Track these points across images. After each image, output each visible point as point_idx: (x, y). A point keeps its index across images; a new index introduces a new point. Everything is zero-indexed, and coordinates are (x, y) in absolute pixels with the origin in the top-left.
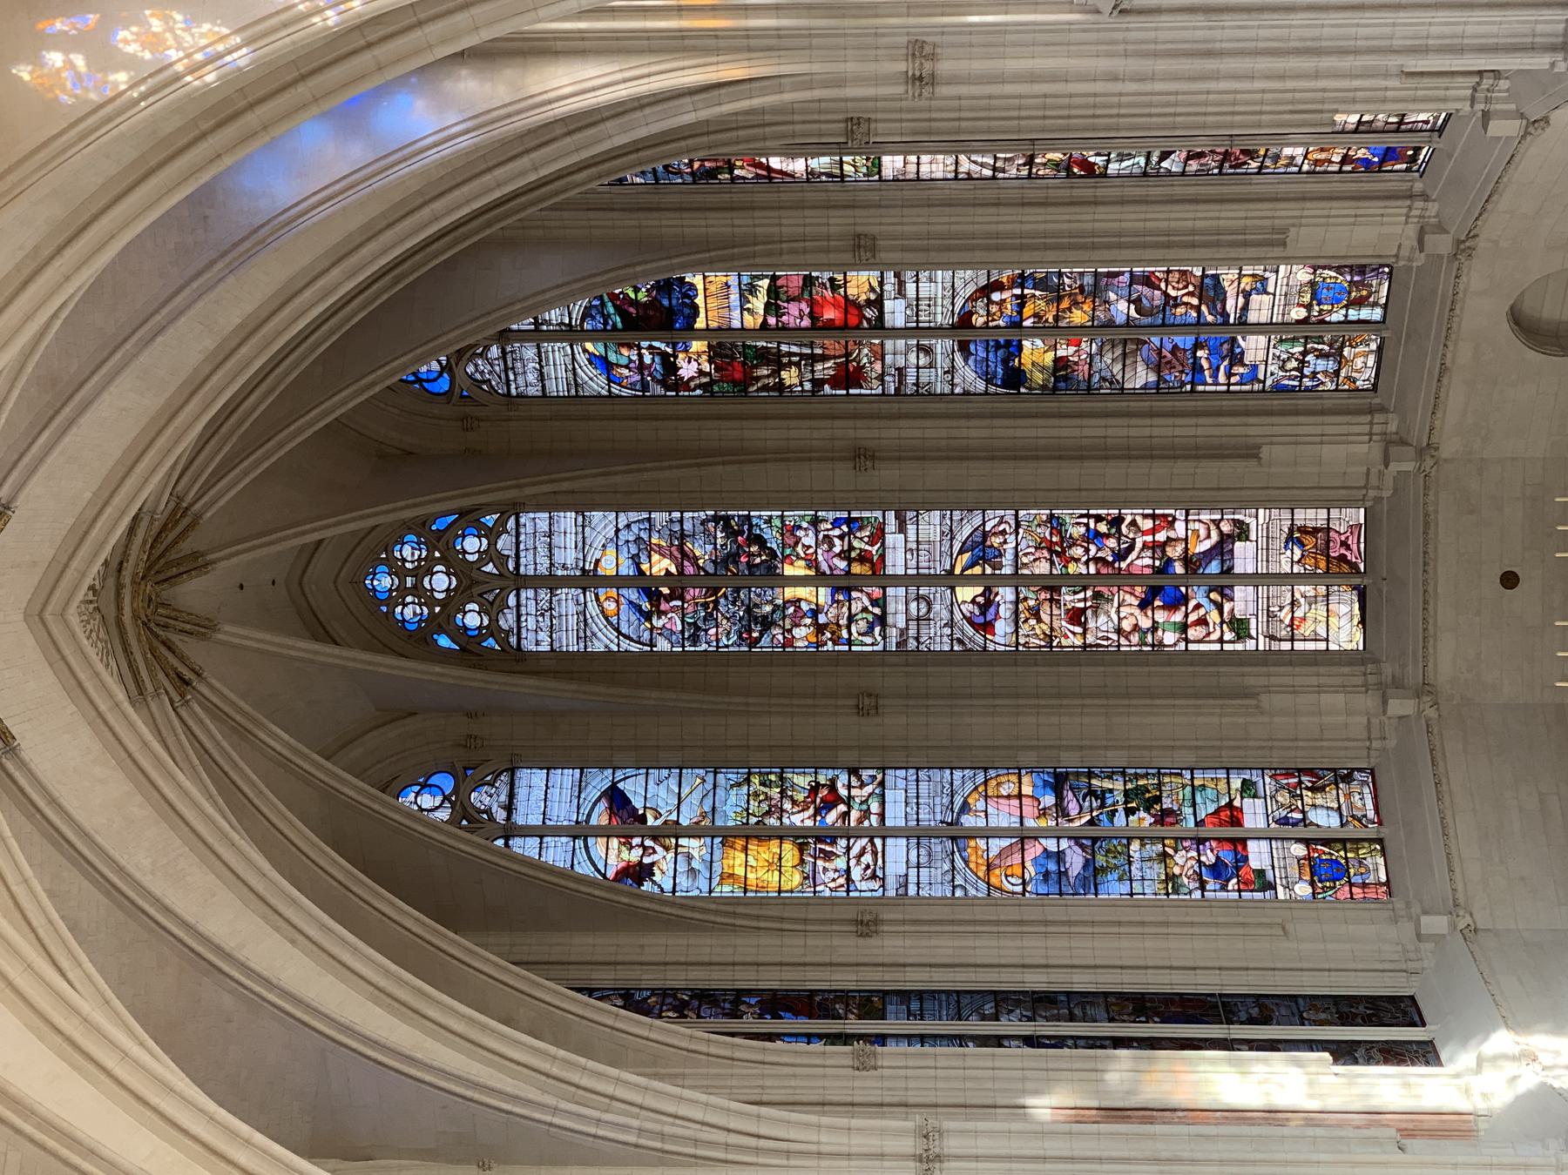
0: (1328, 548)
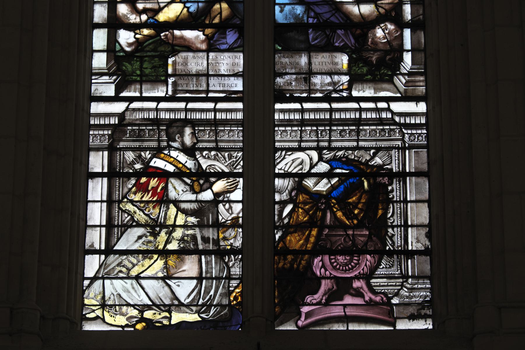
0: (333, 252)
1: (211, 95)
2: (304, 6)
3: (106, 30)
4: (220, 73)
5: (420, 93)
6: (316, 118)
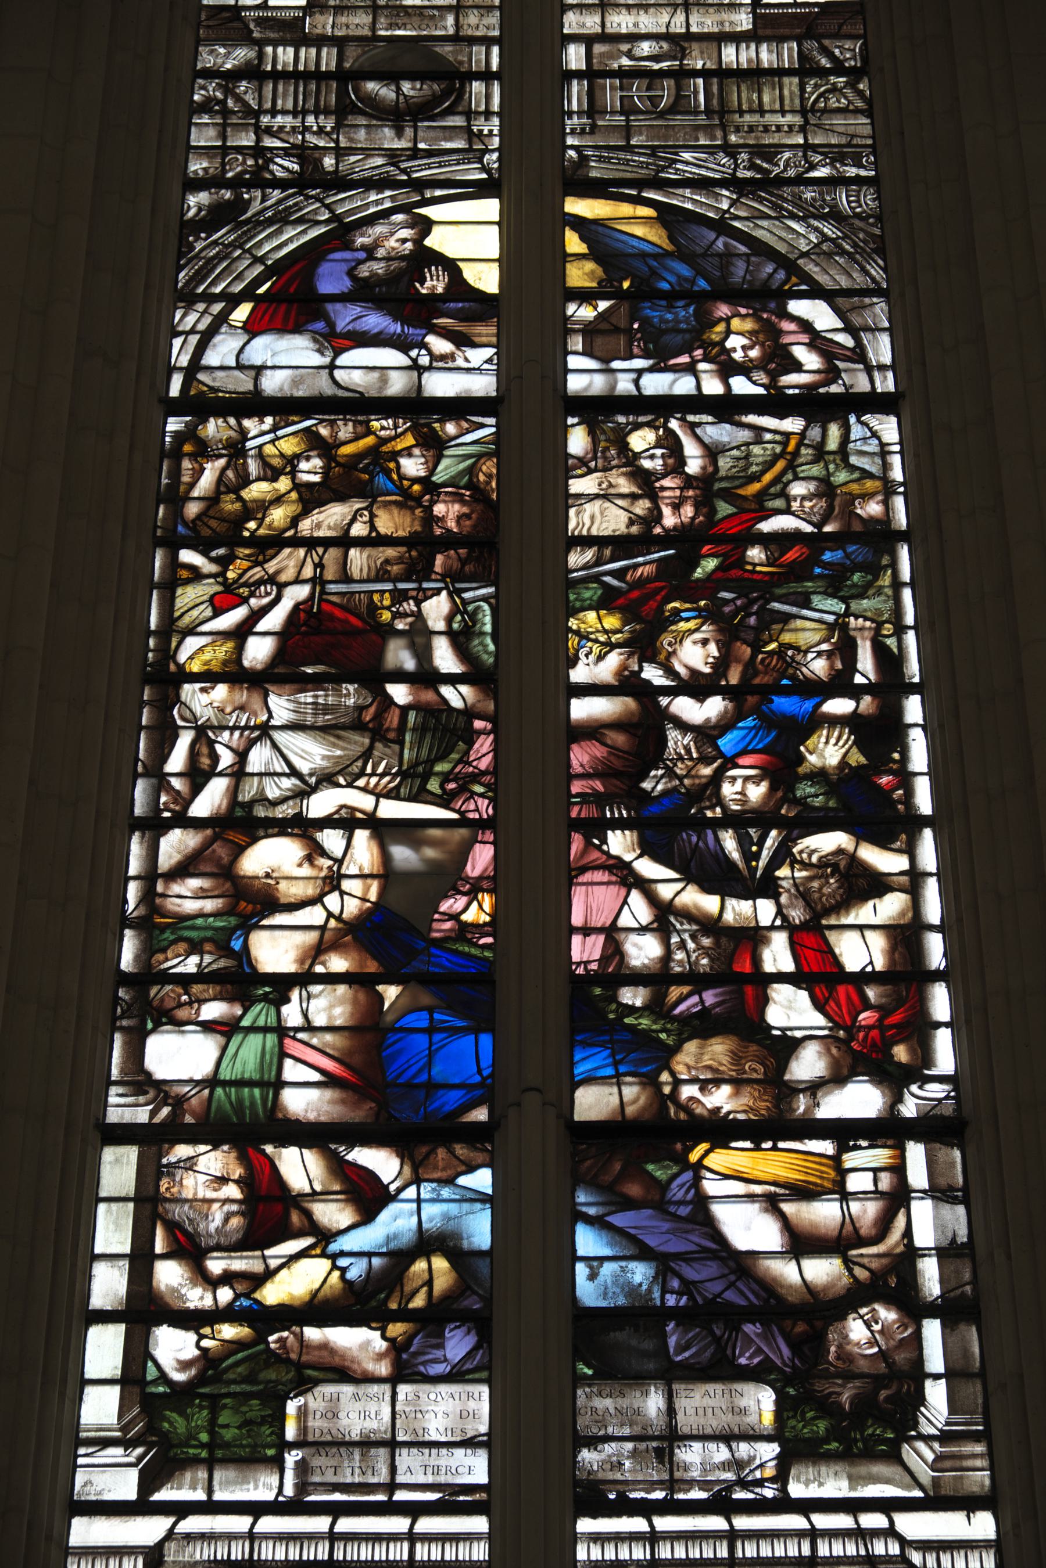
1: (400, 1496)
2: (653, 1264)
3: (122, 1327)
4: (427, 1438)
5: (976, 1489)
6: (691, 1556)
